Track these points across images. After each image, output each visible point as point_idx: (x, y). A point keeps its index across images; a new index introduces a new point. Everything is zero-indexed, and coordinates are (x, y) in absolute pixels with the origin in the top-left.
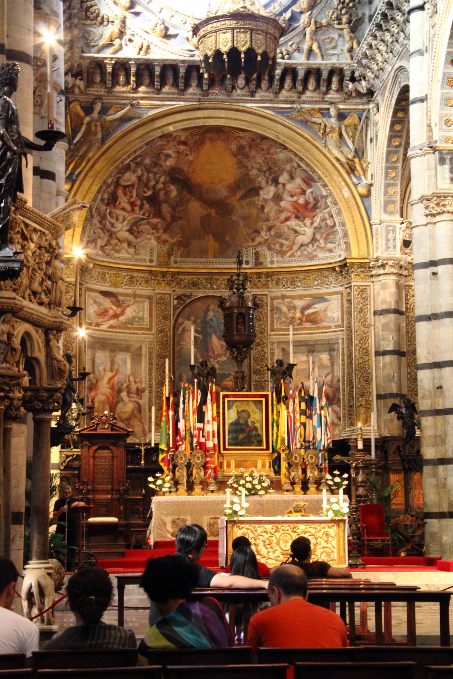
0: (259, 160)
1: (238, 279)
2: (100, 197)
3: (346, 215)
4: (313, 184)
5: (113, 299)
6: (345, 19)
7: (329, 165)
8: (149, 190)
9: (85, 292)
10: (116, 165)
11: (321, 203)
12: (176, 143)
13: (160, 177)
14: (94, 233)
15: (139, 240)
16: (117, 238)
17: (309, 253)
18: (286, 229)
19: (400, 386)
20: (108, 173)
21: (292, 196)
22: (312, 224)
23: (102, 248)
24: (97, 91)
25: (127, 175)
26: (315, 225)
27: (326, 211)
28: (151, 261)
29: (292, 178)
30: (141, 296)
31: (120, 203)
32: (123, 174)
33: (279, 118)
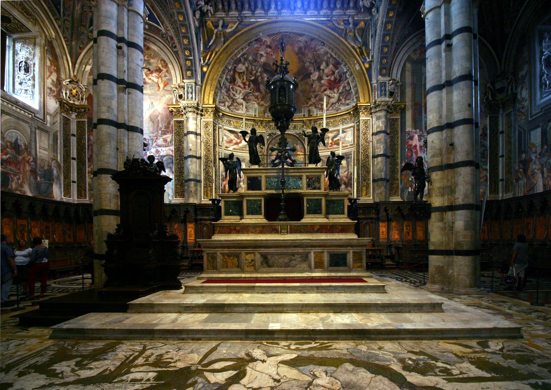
4: (339, 66)
8: (253, 76)
9: (219, 129)
10: (232, 56)
12: (265, 47)
13: (258, 68)
14: (223, 98)
16: (237, 103)
19: (386, 175)
23: (228, 107)
24: (221, 14)
25: (240, 66)
27: (345, 82)
29: (328, 65)
31: (237, 83)
32: (238, 64)
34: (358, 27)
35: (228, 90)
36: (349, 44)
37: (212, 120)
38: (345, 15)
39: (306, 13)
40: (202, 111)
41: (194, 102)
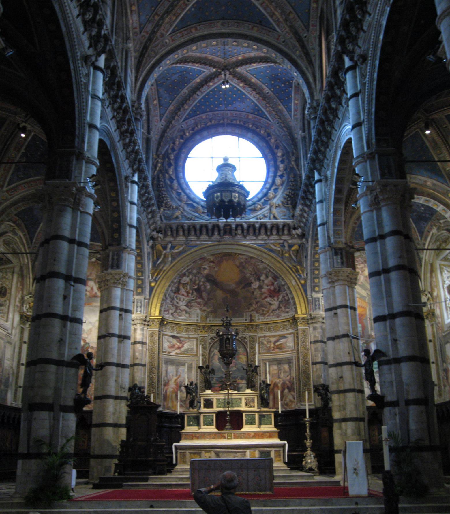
0: (251, 269)
1: (227, 320)
2: (170, 289)
3: (294, 293)
4: (277, 279)
5: (178, 339)
6: (289, 202)
7: (284, 269)
11: (282, 289)
15: (191, 310)
17: (277, 314)
18: (265, 303)
20: (174, 277)
21: (267, 286)
22: (278, 299)
23: (172, 314)
26: (280, 300)
28: (197, 320)
29: (267, 277)
30: (192, 338)
32: (182, 278)
33: (259, 248)
34: (293, 248)
35: (172, 299)
36: (285, 264)
37: (158, 329)
38: (280, 239)
39: (245, 238)
40: (149, 322)
41: (142, 316)
